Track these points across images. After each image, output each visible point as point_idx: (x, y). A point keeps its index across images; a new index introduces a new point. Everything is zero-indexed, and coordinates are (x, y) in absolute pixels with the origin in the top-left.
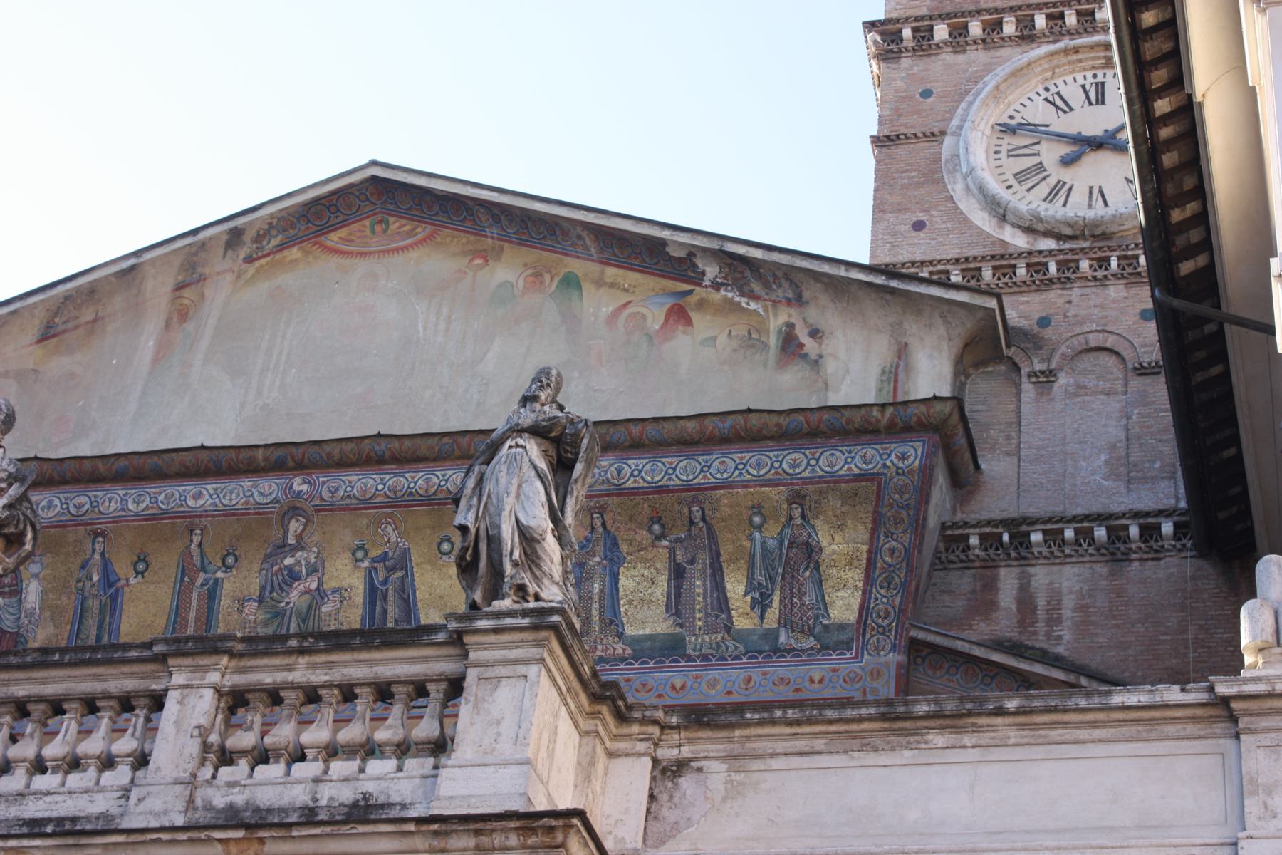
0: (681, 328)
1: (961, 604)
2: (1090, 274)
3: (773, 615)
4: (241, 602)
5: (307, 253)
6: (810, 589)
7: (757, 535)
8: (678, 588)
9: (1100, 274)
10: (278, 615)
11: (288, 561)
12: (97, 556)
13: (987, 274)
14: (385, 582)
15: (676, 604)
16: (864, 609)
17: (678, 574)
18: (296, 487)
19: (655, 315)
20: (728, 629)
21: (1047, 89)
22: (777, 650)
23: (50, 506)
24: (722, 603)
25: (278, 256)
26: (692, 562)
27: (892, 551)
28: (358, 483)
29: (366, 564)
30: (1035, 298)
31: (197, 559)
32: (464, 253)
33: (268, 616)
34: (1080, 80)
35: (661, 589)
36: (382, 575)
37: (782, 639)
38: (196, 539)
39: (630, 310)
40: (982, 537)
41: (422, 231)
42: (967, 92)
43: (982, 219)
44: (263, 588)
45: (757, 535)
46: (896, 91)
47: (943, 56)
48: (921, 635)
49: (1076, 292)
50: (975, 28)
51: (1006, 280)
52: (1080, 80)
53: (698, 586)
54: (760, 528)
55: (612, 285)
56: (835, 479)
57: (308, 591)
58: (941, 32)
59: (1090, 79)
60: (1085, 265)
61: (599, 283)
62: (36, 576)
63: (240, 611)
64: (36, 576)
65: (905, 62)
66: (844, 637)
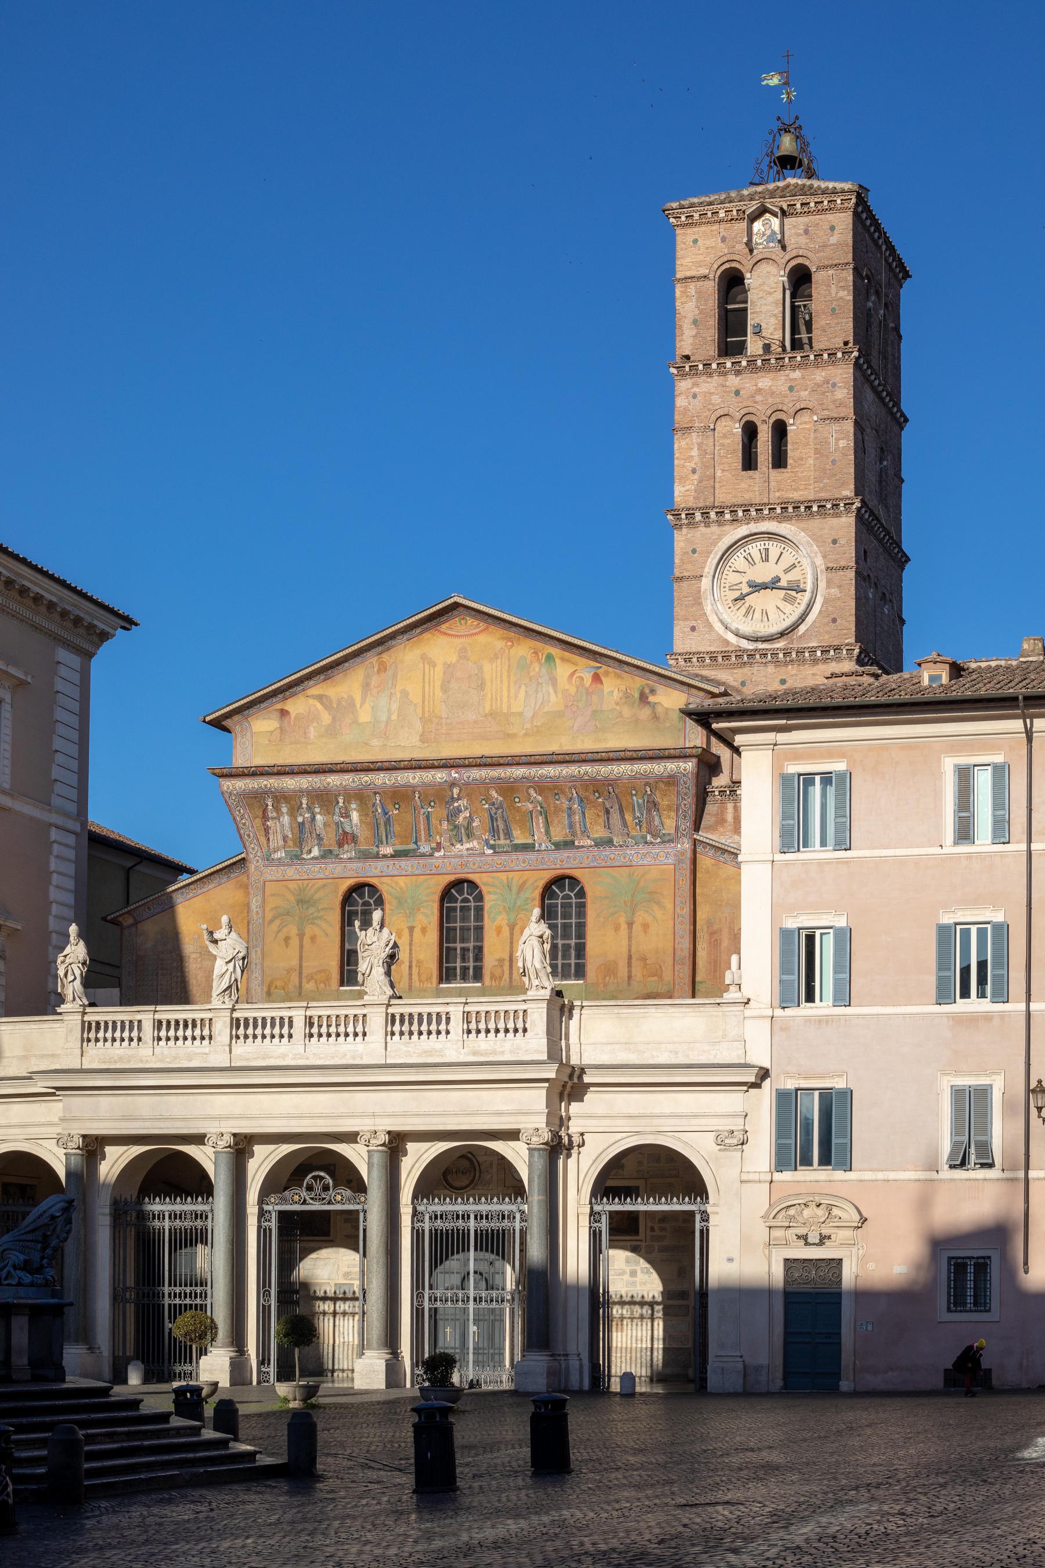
0: (599, 686)
1: (713, 819)
2: (760, 660)
3: (644, 830)
4: (440, 821)
5: (434, 635)
6: (657, 818)
7: (635, 798)
8: (608, 819)
9: (764, 660)
10: (456, 827)
11: (456, 804)
12: (378, 802)
13: (720, 659)
14: (496, 814)
15: (608, 826)
16: (677, 828)
17: (607, 812)
18: (453, 775)
19: (588, 678)
20: (628, 835)
21: (745, 551)
22: (646, 843)
23: (354, 781)
24: (625, 824)
25: (421, 637)
26: (612, 808)
27: (685, 805)
28: (476, 773)
29: (487, 806)
30: (740, 671)
31: (419, 803)
32: (503, 638)
33: (452, 827)
34: (759, 547)
35: (601, 821)
36: (494, 810)
37: (648, 838)
38: (417, 795)
39: (575, 676)
40: (720, 792)
41: (483, 625)
42: (711, 552)
43: (718, 627)
44: (448, 816)
45: (635, 798)
46: (681, 549)
47: (700, 528)
48: (698, 838)
49: (755, 668)
50: (713, 515)
51: (727, 662)
52: (759, 547)
53: (615, 817)
54: (635, 795)
55: (568, 661)
56: (660, 779)
57: (466, 817)
58: (698, 516)
59: (763, 546)
60: (758, 656)
61: (563, 659)
62: (355, 809)
63: (441, 825)
64: (355, 809)
65: (685, 530)
66: (671, 838)
